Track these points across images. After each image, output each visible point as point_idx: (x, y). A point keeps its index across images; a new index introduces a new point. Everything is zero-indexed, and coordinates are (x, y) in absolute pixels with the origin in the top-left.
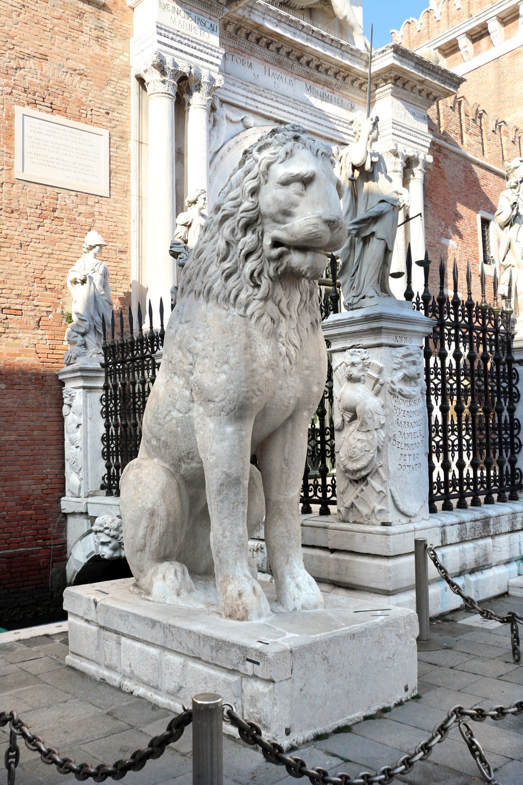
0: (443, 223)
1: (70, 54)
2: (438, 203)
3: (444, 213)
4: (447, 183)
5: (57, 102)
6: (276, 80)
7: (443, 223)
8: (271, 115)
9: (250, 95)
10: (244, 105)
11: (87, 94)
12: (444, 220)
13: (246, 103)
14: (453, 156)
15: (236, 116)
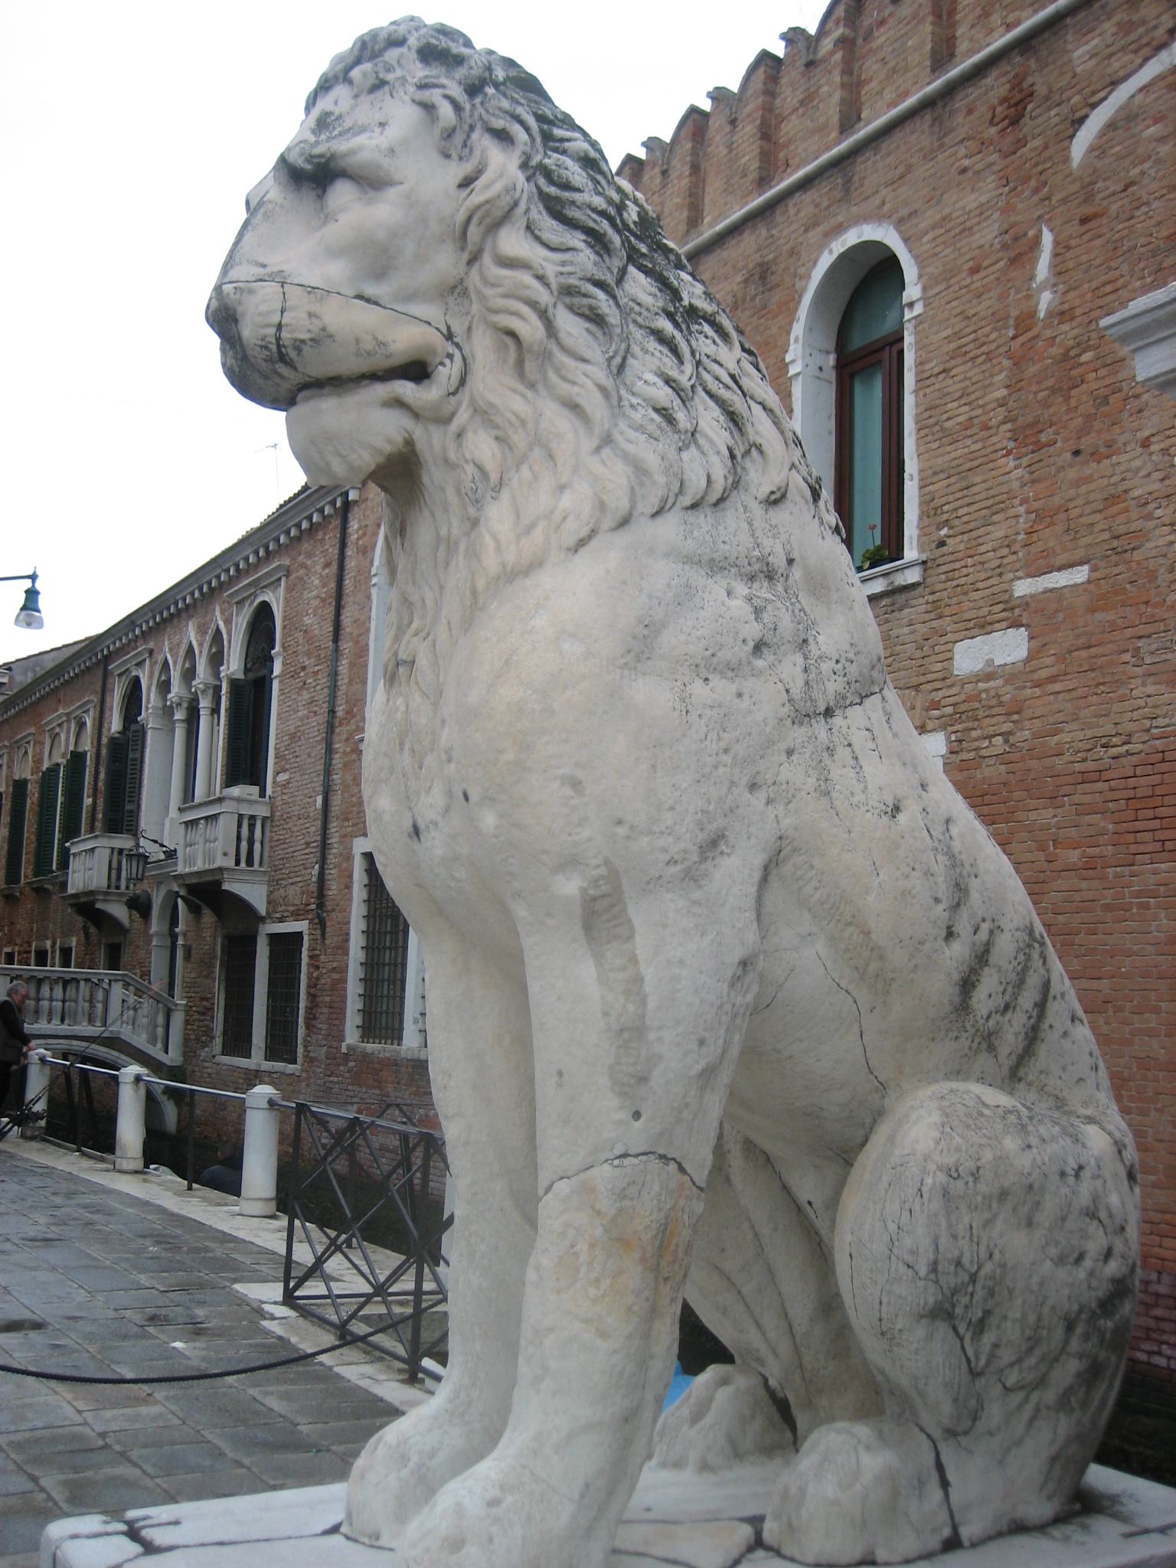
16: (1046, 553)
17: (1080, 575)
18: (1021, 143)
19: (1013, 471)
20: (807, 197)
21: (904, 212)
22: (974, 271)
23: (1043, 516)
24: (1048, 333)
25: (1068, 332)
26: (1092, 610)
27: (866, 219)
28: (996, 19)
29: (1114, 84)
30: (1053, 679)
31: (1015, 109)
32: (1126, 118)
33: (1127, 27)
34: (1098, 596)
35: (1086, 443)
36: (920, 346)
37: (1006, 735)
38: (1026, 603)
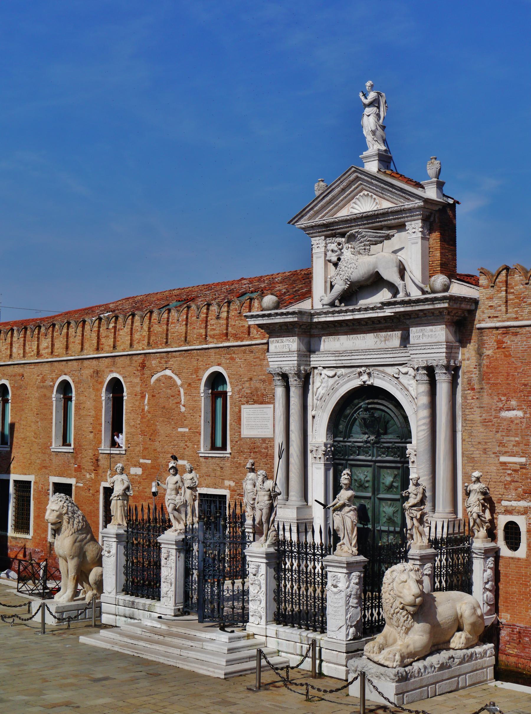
0: (503, 398)
1: (260, 373)
2: (499, 381)
3: (507, 389)
4: (513, 359)
5: (255, 398)
6: (354, 341)
7: (503, 398)
8: (351, 365)
9: (337, 358)
10: (335, 365)
11: (265, 390)
12: (504, 395)
13: (336, 364)
14: (524, 330)
15: (331, 373)
16: (145, 456)
17: (149, 462)
18: (143, 374)
19: (140, 438)
20: (107, 360)
21: (124, 375)
22: (136, 395)
23: (145, 449)
24: (146, 414)
25: (150, 416)
26: (151, 469)
27: (118, 373)
28: (140, 344)
29: (158, 372)
30: (145, 479)
31: (143, 366)
32: (158, 380)
33: (160, 363)
34: (153, 467)
35: (151, 438)
36: (126, 406)
37: (138, 487)
38: (142, 464)
